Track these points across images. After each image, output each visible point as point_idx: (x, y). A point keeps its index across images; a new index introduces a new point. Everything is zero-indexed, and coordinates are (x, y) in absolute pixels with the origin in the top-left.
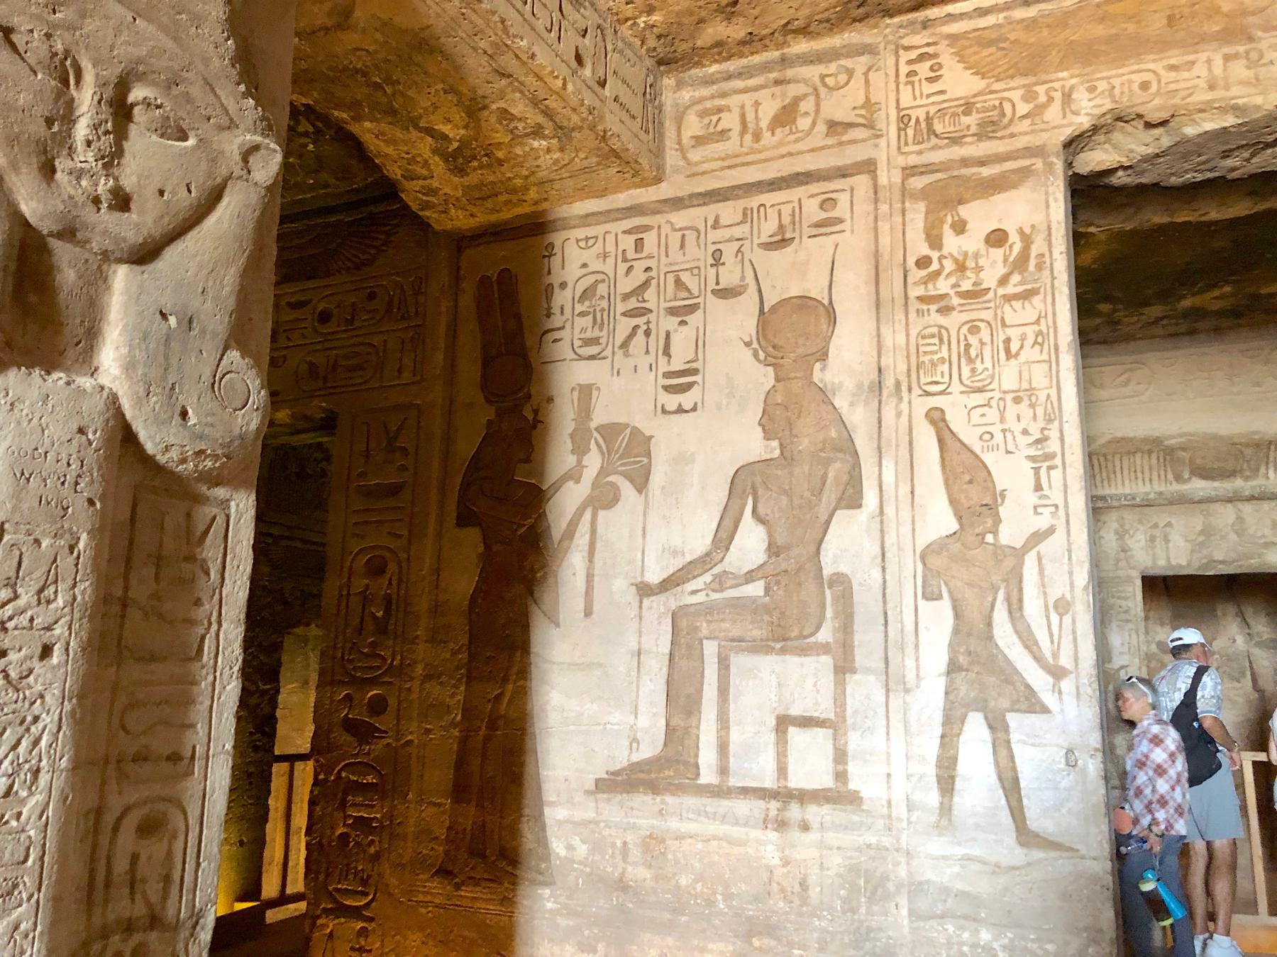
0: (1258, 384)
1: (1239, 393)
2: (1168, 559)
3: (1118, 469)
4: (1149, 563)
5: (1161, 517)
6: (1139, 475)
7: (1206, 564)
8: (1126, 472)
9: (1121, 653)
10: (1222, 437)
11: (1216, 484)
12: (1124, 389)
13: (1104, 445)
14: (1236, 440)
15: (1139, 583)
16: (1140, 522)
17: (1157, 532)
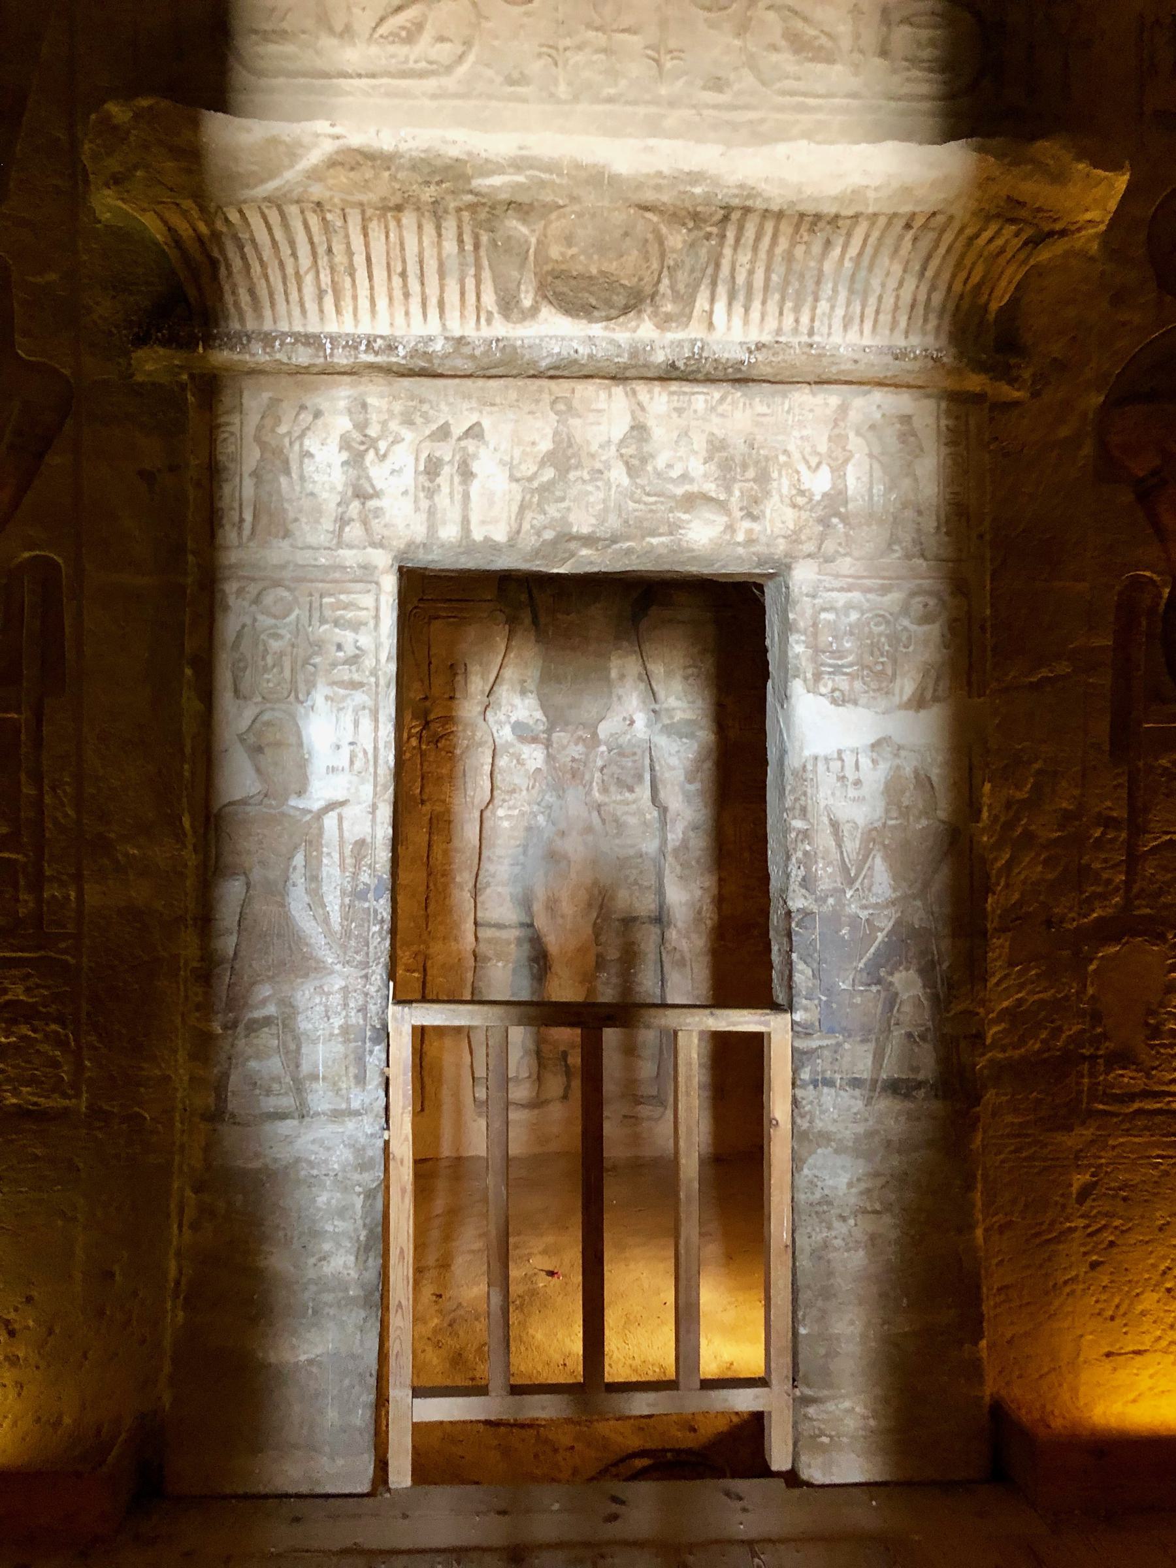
0: (717, 84)
1: (672, 103)
2: (465, 522)
3: (359, 260)
4: (418, 530)
5: (455, 407)
6: (414, 286)
7: (555, 542)
8: (380, 273)
9: (333, 770)
10: (614, 181)
11: (597, 329)
12: (403, 50)
13: (314, 175)
14: (650, 196)
15: (389, 584)
16: (409, 422)
17: (445, 451)
